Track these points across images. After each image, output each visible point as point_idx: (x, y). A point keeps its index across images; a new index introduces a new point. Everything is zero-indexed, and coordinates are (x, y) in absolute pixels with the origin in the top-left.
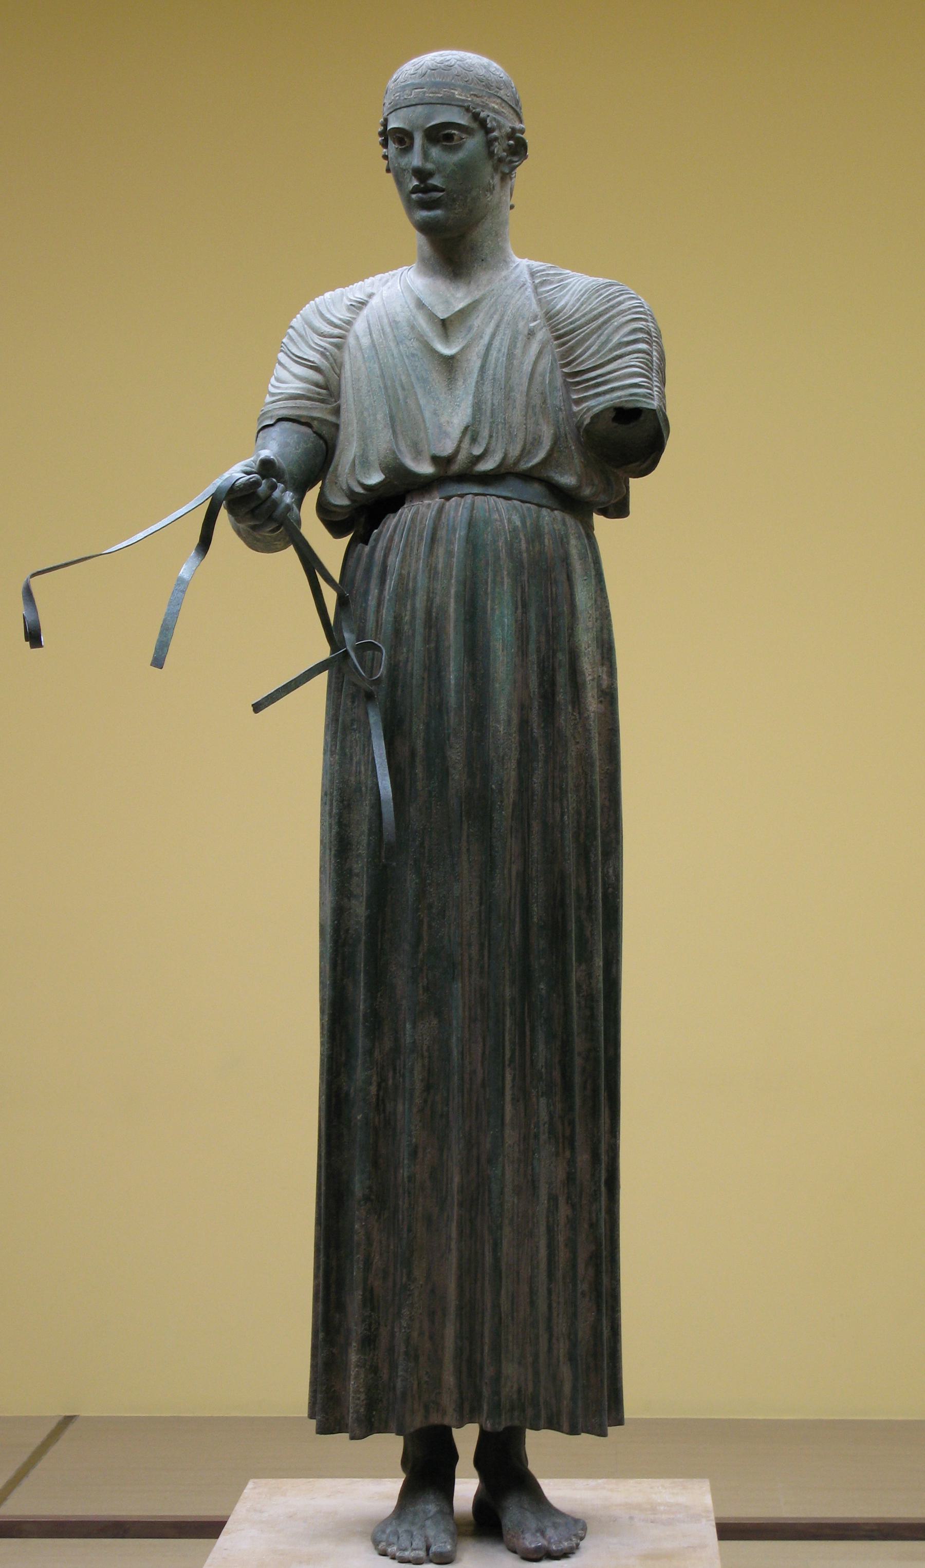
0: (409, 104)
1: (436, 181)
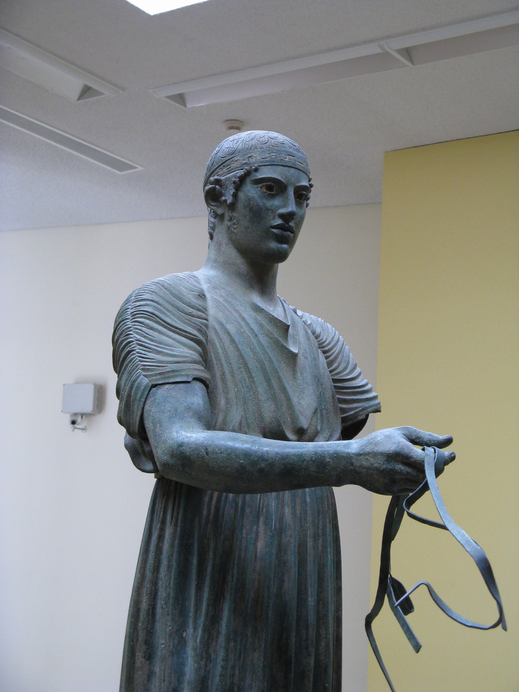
0: (285, 164)
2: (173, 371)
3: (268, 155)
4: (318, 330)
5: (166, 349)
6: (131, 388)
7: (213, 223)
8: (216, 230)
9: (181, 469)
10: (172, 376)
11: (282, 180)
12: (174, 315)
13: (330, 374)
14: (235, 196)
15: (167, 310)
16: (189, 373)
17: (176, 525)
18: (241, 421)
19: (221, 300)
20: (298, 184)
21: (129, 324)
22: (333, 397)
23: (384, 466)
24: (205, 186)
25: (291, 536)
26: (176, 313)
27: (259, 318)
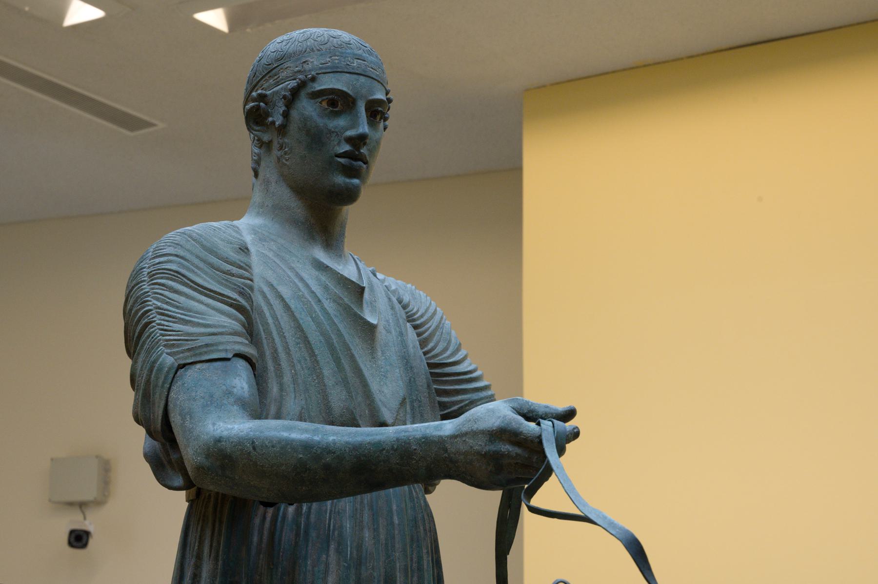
1: (364, 150)
2: (207, 345)
3: (328, 59)
4: (406, 299)
5: (197, 318)
6: (151, 370)
7: (259, 155)
8: (263, 164)
9: (220, 473)
10: (206, 353)
11: (349, 92)
12: (206, 273)
13: (424, 357)
14: (286, 115)
15: (197, 267)
16: (228, 348)
17: (216, 559)
18: (301, 413)
19: (271, 254)
20: (371, 98)
21: (146, 287)
22: (429, 386)
23: (487, 448)
24: (246, 103)
25: (373, 569)
26: (208, 270)
27: (323, 278)
